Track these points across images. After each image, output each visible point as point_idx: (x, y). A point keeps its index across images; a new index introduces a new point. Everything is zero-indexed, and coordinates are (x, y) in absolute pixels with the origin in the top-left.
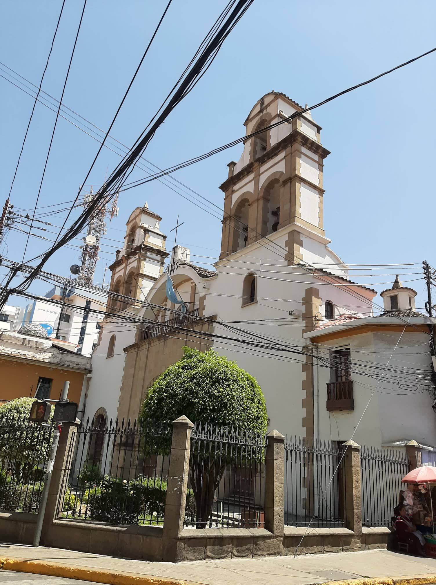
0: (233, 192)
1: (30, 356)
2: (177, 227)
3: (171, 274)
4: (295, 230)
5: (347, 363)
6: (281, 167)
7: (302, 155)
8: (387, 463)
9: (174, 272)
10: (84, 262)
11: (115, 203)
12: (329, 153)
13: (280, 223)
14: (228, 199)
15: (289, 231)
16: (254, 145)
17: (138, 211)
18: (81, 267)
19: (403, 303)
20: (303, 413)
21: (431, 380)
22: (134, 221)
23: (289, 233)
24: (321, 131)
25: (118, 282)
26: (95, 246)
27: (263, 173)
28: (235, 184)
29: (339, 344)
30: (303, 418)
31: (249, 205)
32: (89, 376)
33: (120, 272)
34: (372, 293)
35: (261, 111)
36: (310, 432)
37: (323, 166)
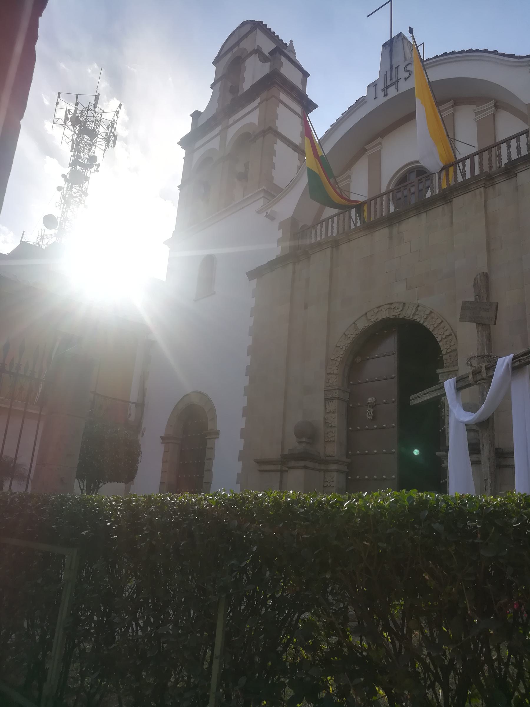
3: (386, 95)
9: (397, 88)
18: (59, 219)
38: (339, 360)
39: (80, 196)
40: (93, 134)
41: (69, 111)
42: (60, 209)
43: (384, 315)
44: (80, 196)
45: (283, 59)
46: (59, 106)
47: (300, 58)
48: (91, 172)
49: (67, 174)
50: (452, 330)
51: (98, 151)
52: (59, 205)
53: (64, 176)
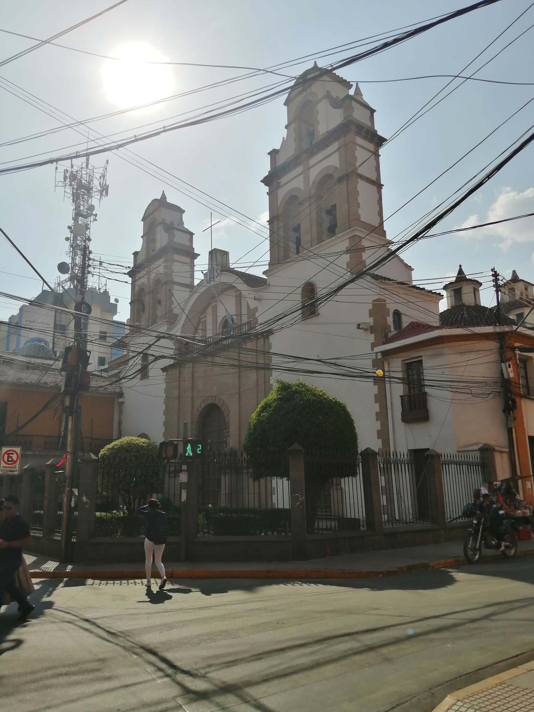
1: (52, 384)
2: (211, 226)
4: (355, 235)
5: (420, 373)
6: (335, 161)
8: (464, 466)
10: (73, 259)
11: (104, 179)
13: (338, 227)
15: (349, 237)
18: (70, 265)
19: (468, 299)
20: (378, 425)
21: (502, 386)
22: (152, 216)
23: (349, 238)
24: (375, 114)
26: (85, 237)
27: (313, 166)
28: (280, 177)
30: (378, 431)
31: (300, 204)
32: (121, 400)
34: (438, 296)
36: (386, 443)
37: (380, 155)
38: (196, 422)
39: (85, 242)
40: (89, 189)
41: (67, 170)
42: (70, 257)
43: (210, 402)
44: (85, 242)
45: (175, 232)
46: (57, 171)
47: (188, 224)
48: (91, 221)
49: (72, 225)
50: (229, 412)
51: (94, 201)
52: (69, 253)
53: (69, 228)
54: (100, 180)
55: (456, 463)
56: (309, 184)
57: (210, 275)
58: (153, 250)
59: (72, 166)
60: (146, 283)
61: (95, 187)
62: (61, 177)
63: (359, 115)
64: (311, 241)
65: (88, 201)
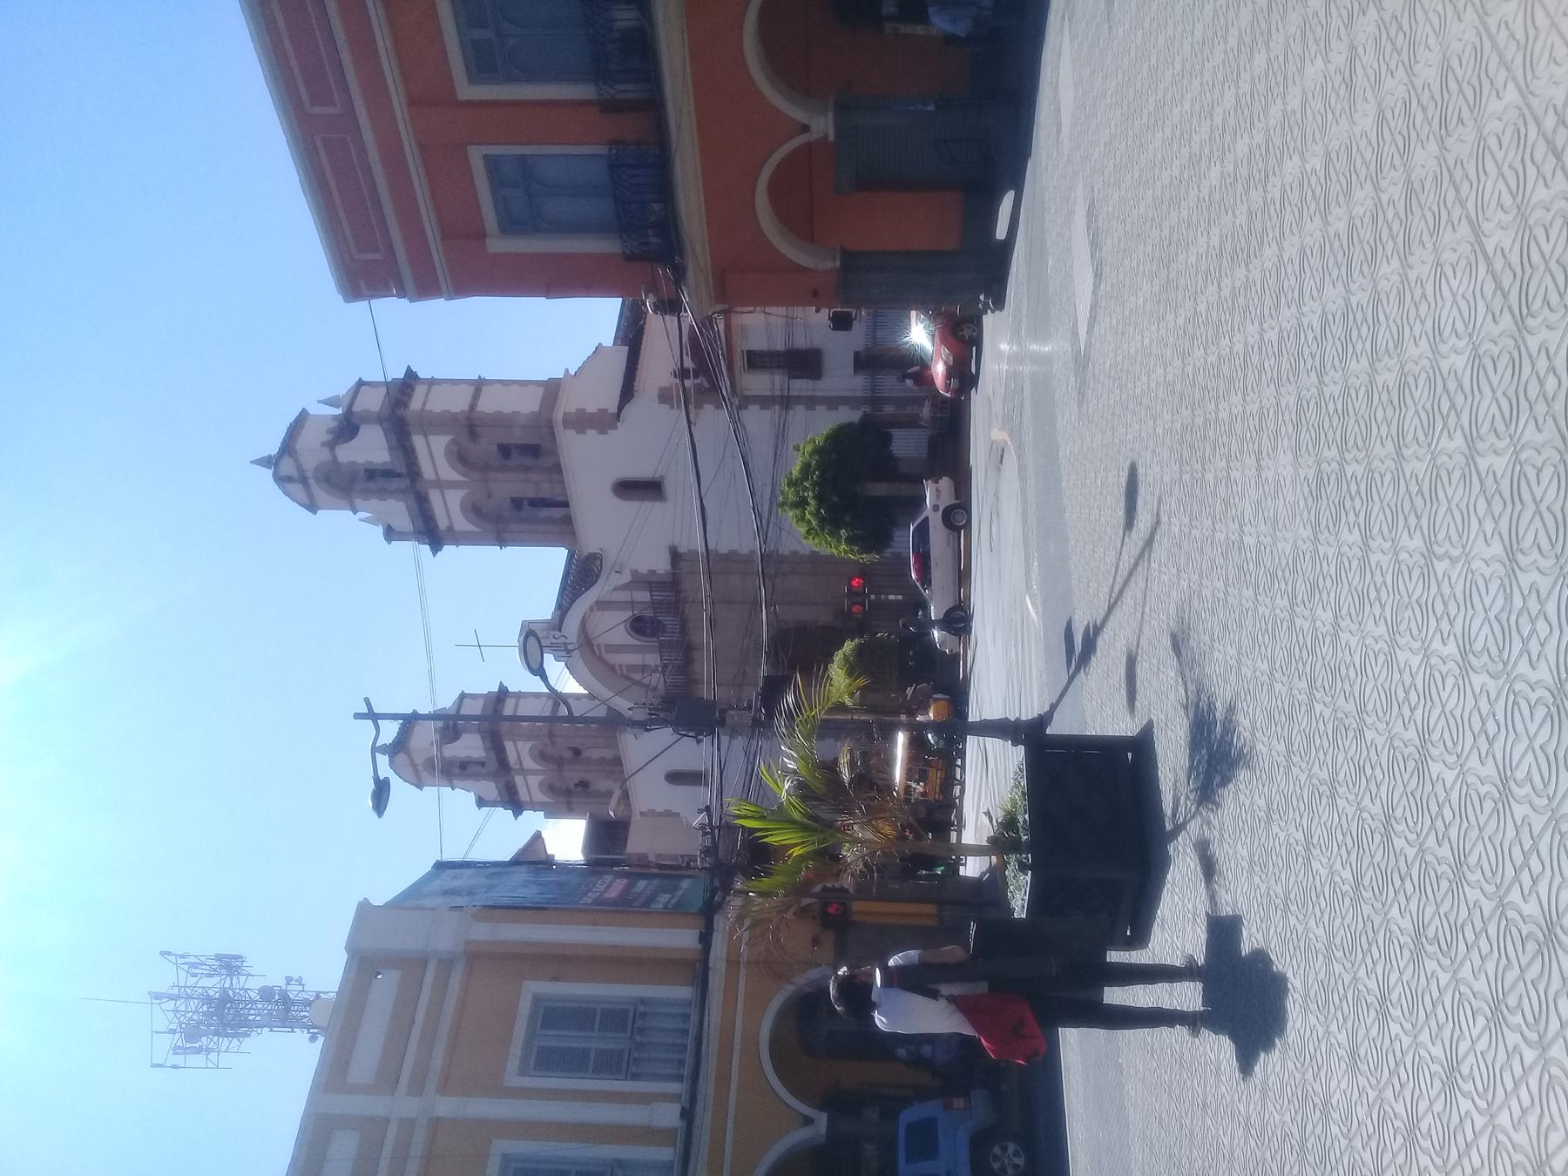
0: (450, 529)
5: (762, 354)
6: (440, 443)
7: (427, 408)
12: (408, 366)
14: (459, 538)
16: (367, 494)
17: (401, 758)
20: (821, 409)
22: (420, 768)
25: (551, 789)
27: (436, 473)
28: (436, 526)
29: (739, 362)
33: (530, 785)
35: (304, 481)
49: (309, 1033)
54: (199, 975)
55: (875, 331)
56: (462, 481)
57: (564, 652)
58: (483, 764)
59: (173, 1032)
60: (541, 778)
61: (222, 982)
62: (199, 1060)
63: (373, 402)
64: (551, 482)
65: (253, 1002)
